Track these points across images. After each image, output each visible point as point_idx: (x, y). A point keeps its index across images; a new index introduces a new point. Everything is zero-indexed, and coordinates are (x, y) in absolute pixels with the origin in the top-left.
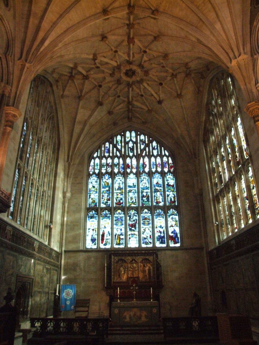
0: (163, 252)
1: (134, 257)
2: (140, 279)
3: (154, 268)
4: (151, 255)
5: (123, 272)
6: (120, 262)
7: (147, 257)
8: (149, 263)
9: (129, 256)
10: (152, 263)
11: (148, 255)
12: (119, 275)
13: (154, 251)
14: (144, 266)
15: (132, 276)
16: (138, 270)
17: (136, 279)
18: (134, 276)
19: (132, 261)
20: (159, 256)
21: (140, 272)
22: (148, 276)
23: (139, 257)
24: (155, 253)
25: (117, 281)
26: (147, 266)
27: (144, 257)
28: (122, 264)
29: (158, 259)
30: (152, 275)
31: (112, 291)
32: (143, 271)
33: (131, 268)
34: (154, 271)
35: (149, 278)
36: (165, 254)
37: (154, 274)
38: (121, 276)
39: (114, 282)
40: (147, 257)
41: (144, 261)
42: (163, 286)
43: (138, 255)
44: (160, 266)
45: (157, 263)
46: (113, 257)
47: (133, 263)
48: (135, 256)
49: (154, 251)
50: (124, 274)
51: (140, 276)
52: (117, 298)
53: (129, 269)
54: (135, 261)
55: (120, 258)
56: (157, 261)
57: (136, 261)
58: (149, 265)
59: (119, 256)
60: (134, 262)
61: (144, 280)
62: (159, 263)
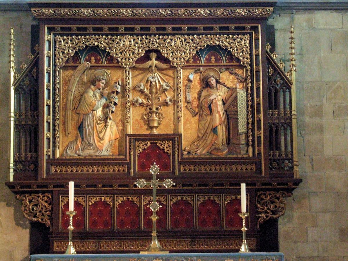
0: (301, 18)
1: (155, 41)
2: (185, 144)
3: (251, 94)
4: (240, 30)
5: (99, 113)
6: (84, 64)
7: (223, 41)
8: (228, 68)
9: (130, 31)
10: (242, 67)
11: (225, 30)
12: (80, 128)
13: (258, 11)
14: (206, 84)
15: (144, 131)
16: (175, 102)
17: (166, 146)
18: (155, 132)
19: (147, 57)
20: (279, 38)
21: (184, 114)
22: (222, 131)
23: (178, 41)
24: (263, 19)
25: (71, 153)
26: (217, 82)
27: (205, 41)
28: (99, 72)
29: (273, 50)
30: (242, 128)
31: (43, 201)
32: (200, 106)
33: (142, 92)
34: (251, 108)
35: (229, 142)
36: (312, 28)
37: (252, 125)
38: (88, 129)
39: (53, 161)
40: (223, 41)
41: (203, 62)
42: (298, 182)
43: (177, 31)
44: (287, 85)
45: (271, 71)
46: (47, 37)
47: (149, 70)
48: (161, 31)
49: (258, 11)
50: (106, 118)
51: (182, 131)
52: (64, 237)
53: (131, 96)
54: (160, 58)
55: (84, 41)
56: (269, 62)
57: (166, 61)
58: (227, 78)
59: (82, 31)
60: (154, 62)
61: (202, 152)
62: (277, 71)
